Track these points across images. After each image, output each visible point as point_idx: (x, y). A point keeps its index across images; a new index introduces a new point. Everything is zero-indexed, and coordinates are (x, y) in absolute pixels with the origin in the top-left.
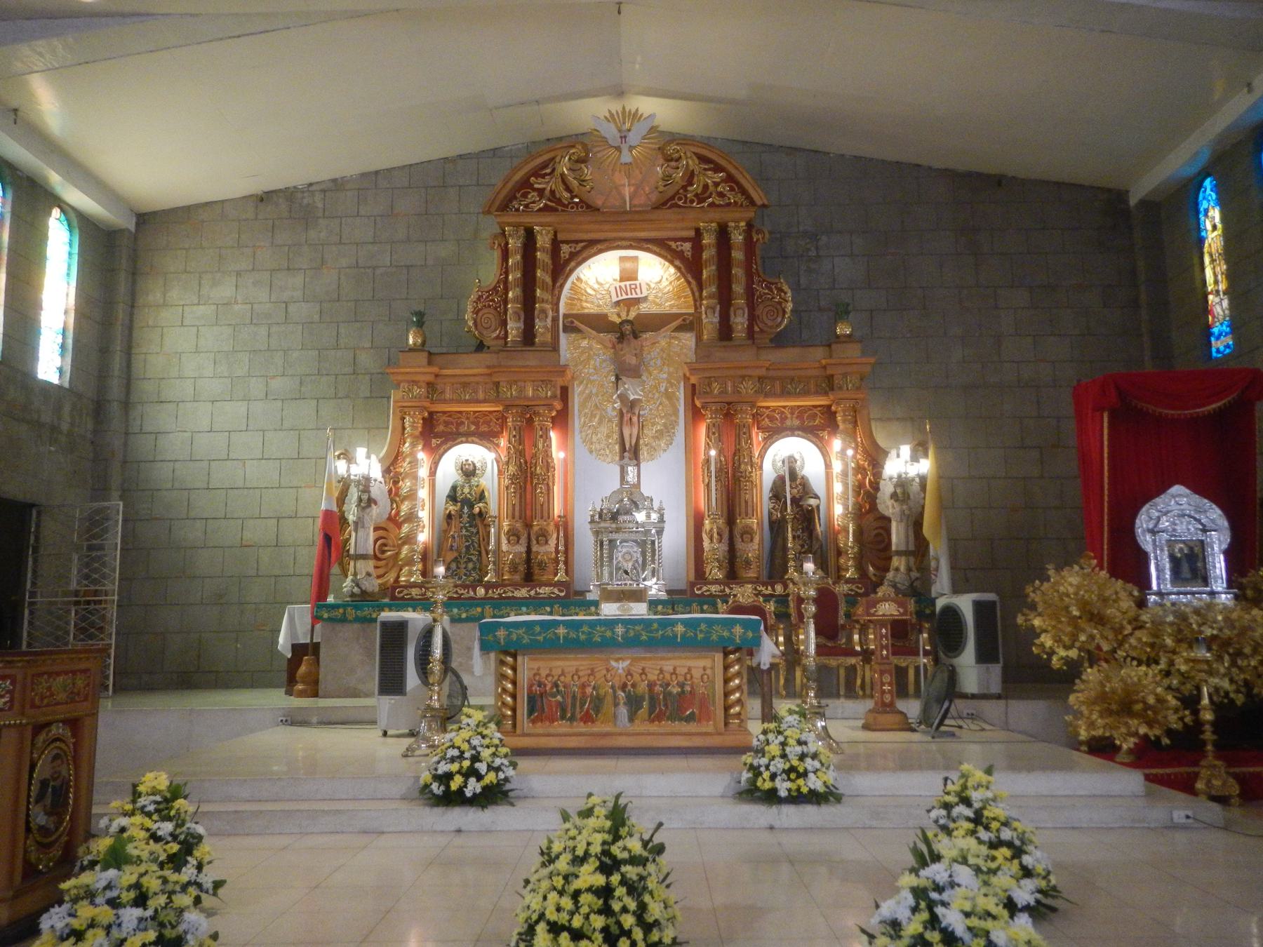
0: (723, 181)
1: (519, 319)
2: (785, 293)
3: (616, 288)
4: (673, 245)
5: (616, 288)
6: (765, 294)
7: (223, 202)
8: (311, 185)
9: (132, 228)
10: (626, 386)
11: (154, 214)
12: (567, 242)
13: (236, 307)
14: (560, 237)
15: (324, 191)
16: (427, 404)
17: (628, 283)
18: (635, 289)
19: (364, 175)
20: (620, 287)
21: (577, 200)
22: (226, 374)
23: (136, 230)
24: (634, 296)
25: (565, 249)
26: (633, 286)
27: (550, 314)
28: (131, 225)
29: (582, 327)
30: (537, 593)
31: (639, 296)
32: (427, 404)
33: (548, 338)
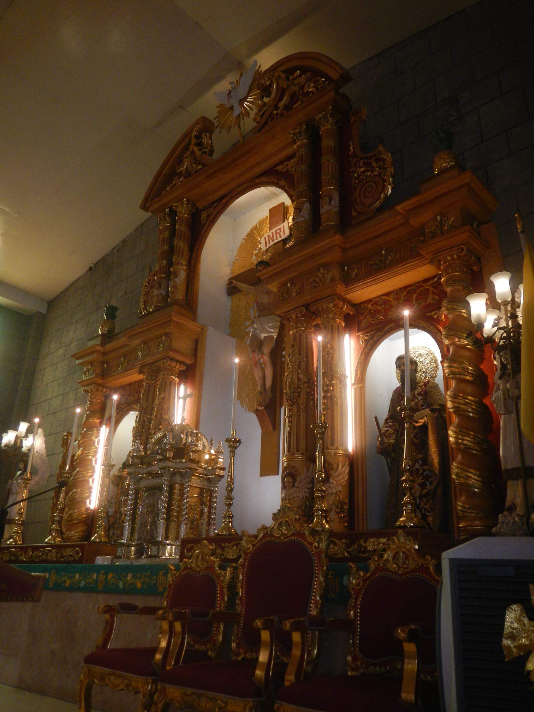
0: (309, 80)
1: (160, 286)
2: (384, 160)
3: (265, 238)
4: (280, 168)
5: (265, 238)
6: (363, 172)
7: (78, 279)
8: (113, 249)
9: (44, 311)
10: (255, 326)
11: (54, 299)
12: (205, 209)
13: (73, 345)
14: (200, 206)
15: (118, 250)
16: (100, 381)
17: (274, 230)
18: (279, 233)
19: (136, 230)
20: (269, 236)
21: (200, 167)
22: (62, 393)
23: (47, 312)
24: (279, 239)
25: (204, 215)
26: (278, 231)
27: (182, 274)
28: (43, 310)
29: (240, 285)
30: (62, 557)
31: (283, 237)
32: (100, 381)
33: (180, 296)
